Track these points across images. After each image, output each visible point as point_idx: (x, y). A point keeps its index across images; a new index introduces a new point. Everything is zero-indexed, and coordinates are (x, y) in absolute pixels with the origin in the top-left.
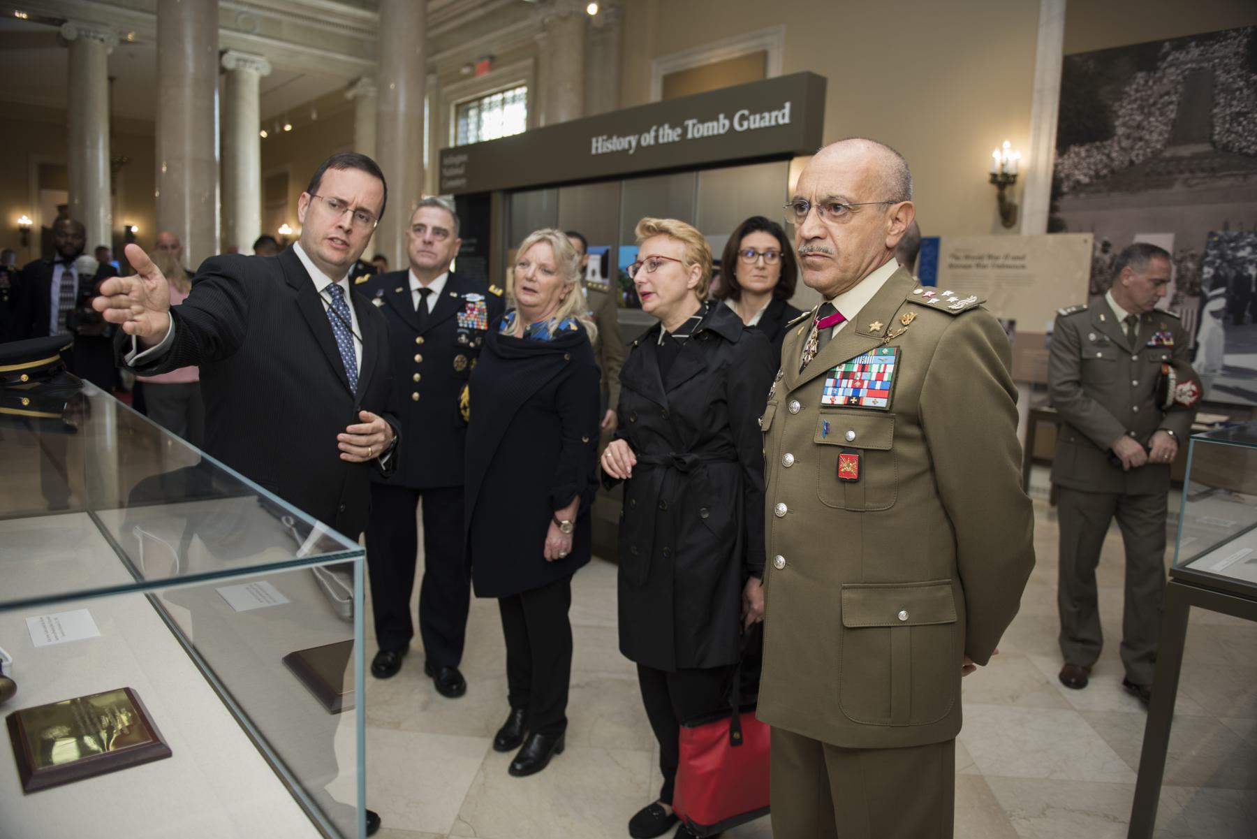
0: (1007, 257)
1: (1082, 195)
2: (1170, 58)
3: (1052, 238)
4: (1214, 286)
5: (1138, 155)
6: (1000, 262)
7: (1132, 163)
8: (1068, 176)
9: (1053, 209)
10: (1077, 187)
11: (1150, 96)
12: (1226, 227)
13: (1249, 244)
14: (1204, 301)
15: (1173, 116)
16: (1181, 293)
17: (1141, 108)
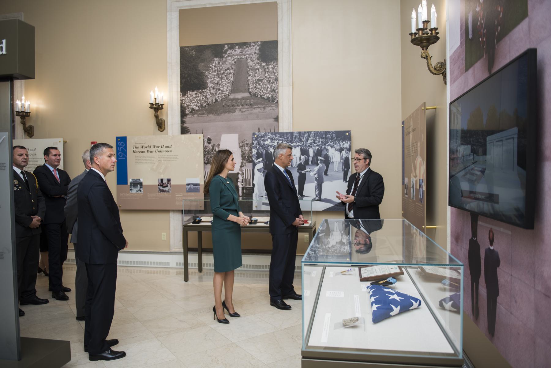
0: (162, 146)
1: (196, 115)
2: (228, 52)
3: (183, 135)
4: (258, 158)
5: (219, 97)
6: (159, 149)
7: (216, 100)
8: (188, 106)
9: (183, 122)
10: (193, 111)
11: (221, 70)
12: (259, 131)
13: (269, 138)
14: (254, 165)
15: (232, 79)
16: (244, 162)
17: (218, 75)
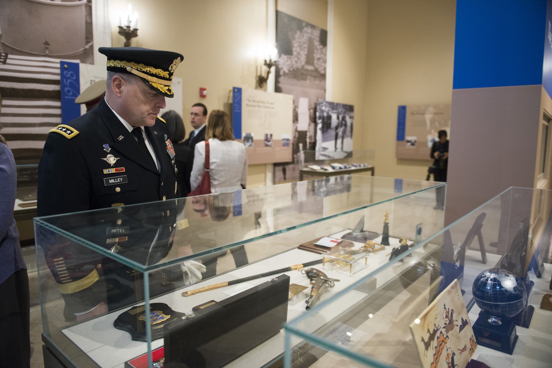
0: (268, 103)
6: (266, 105)
